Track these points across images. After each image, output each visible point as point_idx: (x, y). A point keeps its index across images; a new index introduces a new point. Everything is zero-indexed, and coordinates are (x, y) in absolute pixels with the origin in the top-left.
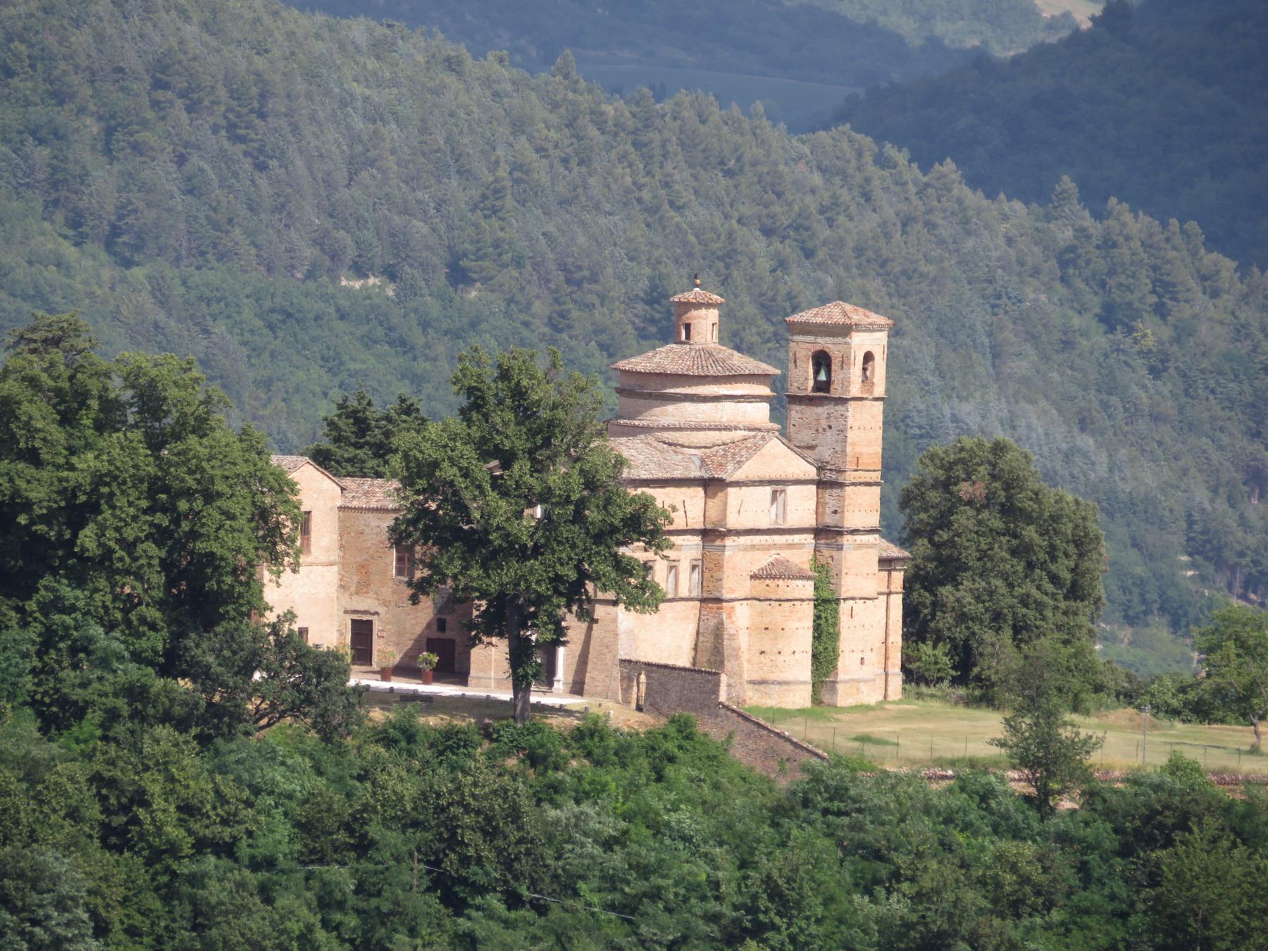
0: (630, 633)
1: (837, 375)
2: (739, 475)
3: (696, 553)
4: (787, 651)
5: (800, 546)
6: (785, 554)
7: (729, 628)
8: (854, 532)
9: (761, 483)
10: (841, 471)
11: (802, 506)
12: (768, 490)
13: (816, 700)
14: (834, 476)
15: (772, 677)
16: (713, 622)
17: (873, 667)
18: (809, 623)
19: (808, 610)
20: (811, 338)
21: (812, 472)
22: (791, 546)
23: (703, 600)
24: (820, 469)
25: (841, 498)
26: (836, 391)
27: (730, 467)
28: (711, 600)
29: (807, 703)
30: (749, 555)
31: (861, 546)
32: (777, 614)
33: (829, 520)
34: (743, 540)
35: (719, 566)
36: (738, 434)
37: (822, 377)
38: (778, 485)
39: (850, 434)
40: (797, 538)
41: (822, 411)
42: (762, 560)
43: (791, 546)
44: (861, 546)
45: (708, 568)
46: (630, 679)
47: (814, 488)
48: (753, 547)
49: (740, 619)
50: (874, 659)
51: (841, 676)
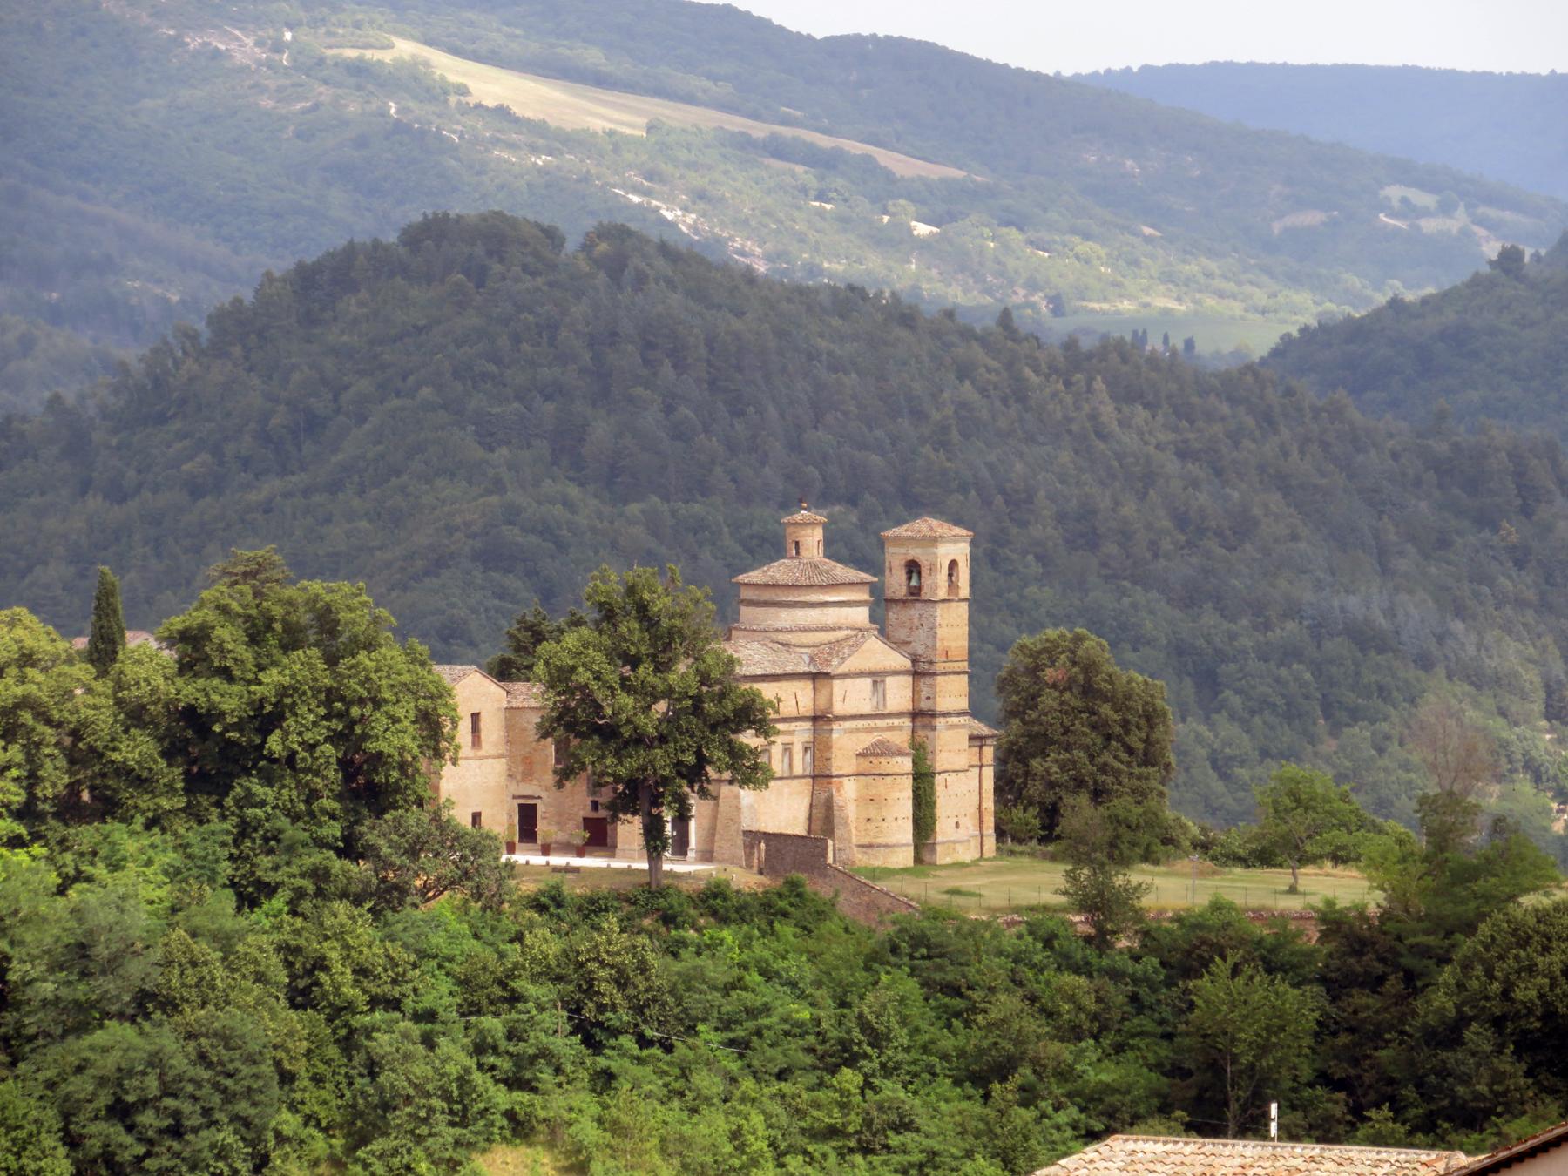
0: (751, 806)
1: (927, 581)
2: (843, 669)
3: (808, 737)
4: (890, 819)
5: (900, 728)
6: (887, 736)
8: (946, 714)
9: (861, 674)
10: (931, 663)
11: (899, 694)
12: (869, 681)
13: (918, 859)
15: (879, 841)
16: (824, 796)
17: (969, 827)
18: (908, 794)
19: (908, 783)
20: (903, 550)
21: (908, 664)
22: (891, 728)
23: (814, 777)
24: (915, 662)
25: (933, 686)
26: (926, 594)
27: (835, 662)
28: (820, 776)
29: (910, 863)
30: (854, 737)
31: (953, 726)
32: (881, 786)
33: (924, 705)
34: (848, 724)
35: (829, 747)
36: (843, 633)
37: (914, 583)
38: (877, 677)
39: (939, 631)
40: (896, 722)
41: (915, 612)
42: (866, 740)
43: (891, 728)
44: (953, 726)
45: (818, 748)
46: (752, 847)
47: (910, 679)
48: (858, 730)
49: (848, 793)
51: (939, 838)
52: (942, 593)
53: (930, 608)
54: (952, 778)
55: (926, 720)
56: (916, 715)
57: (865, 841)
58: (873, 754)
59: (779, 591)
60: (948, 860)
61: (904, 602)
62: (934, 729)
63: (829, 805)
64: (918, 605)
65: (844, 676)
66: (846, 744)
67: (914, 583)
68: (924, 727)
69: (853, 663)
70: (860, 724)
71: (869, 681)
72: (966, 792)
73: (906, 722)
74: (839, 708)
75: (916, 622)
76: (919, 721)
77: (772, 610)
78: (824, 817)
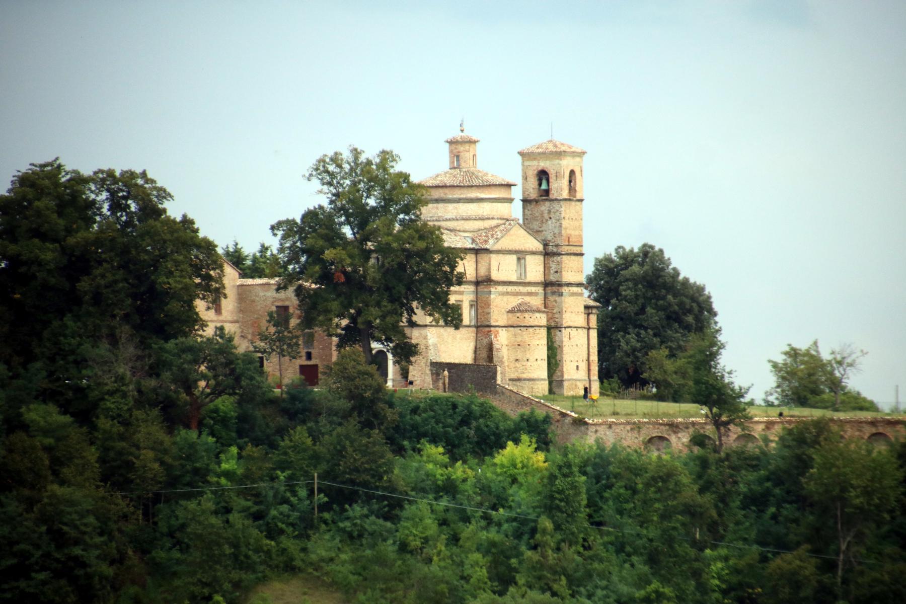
0: (435, 345)
1: (554, 185)
2: (497, 247)
3: (472, 297)
4: (532, 359)
5: (536, 294)
6: (527, 299)
7: (496, 345)
8: (569, 284)
9: (510, 252)
10: (557, 246)
11: (535, 269)
12: (514, 257)
13: (551, 391)
14: (555, 250)
15: (524, 376)
16: (485, 341)
17: (582, 374)
18: (544, 342)
19: (544, 332)
20: (535, 163)
21: (540, 247)
22: (530, 294)
23: (477, 327)
24: (546, 245)
25: (559, 263)
26: (553, 194)
27: (491, 241)
28: (483, 327)
29: (547, 393)
30: (505, 298)
31: (573, 294)
32: (526, 335)
33: (553, 278)
34: (500, 288)
35: (488, 305)
36: (494, 223)
37: (544, 187)
38: (521, 255)
39: (565, 223)
40: (533, 289)
41: (545, 207)
42: (514, 302)
43: (530, 294)
44: (573, 294)
45: (480, 305)
46: (438, 374)
47: (542, 258)
48: (508, 293)
49: (502, 339)
50: (583, 366)
51: (566, 377)
52: (565, 194)
53: (556, 205)
54: (574, 332)
55: (555, 289)
56: (547, 284)
57: (513, 376)
58: (519, 311)
59: (446, 191)
60: (571, 393)
61: (537, 201)
62: (561, 295)
63: (490, 348)
64: (547, 203)
65: (499, 252)
66: (500, 304)
67: (544, 187)
68: (553, 293)
69: (504, 244)
70: (510, 289)
71: (514, 257)
72: (580, 350)
73: (540, 290)
74: (495, 276)
75: (546, 216)
76: (549, 289)
77: (441, 205)
78: (486, 353)
